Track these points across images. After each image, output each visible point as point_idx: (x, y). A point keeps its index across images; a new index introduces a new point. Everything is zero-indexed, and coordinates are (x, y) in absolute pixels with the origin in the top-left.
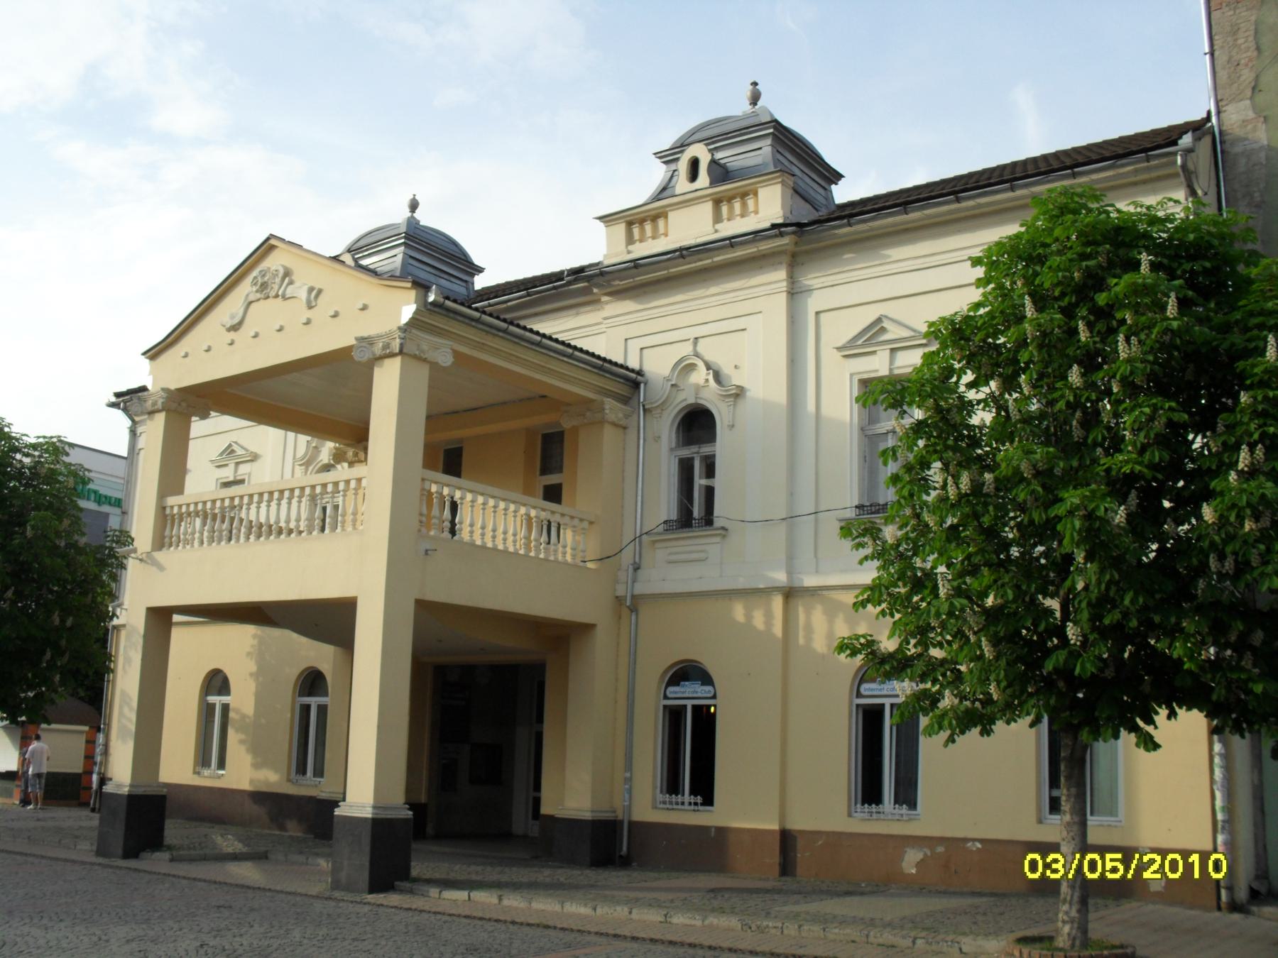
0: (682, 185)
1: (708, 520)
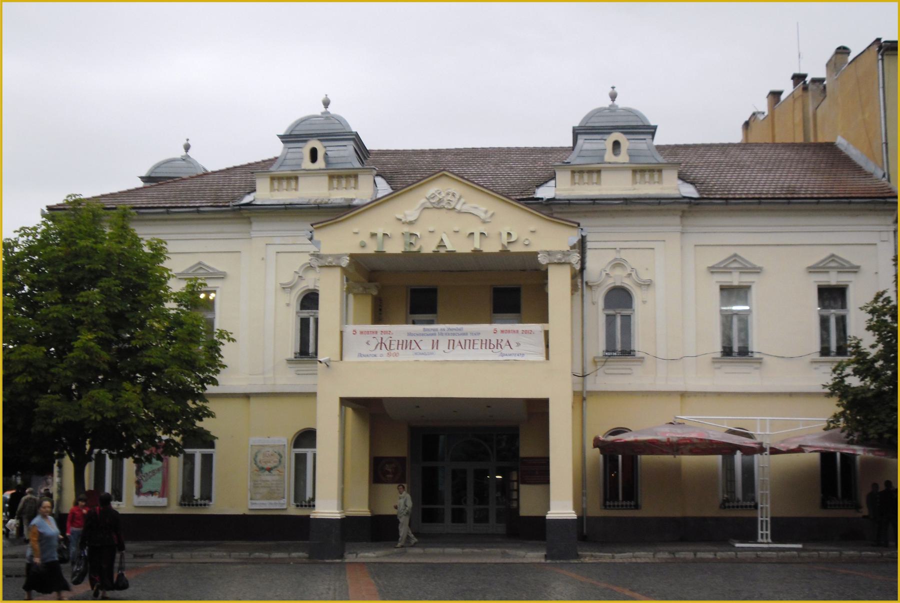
0: (609, 157)
1: (627, 352)
